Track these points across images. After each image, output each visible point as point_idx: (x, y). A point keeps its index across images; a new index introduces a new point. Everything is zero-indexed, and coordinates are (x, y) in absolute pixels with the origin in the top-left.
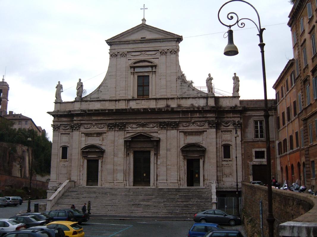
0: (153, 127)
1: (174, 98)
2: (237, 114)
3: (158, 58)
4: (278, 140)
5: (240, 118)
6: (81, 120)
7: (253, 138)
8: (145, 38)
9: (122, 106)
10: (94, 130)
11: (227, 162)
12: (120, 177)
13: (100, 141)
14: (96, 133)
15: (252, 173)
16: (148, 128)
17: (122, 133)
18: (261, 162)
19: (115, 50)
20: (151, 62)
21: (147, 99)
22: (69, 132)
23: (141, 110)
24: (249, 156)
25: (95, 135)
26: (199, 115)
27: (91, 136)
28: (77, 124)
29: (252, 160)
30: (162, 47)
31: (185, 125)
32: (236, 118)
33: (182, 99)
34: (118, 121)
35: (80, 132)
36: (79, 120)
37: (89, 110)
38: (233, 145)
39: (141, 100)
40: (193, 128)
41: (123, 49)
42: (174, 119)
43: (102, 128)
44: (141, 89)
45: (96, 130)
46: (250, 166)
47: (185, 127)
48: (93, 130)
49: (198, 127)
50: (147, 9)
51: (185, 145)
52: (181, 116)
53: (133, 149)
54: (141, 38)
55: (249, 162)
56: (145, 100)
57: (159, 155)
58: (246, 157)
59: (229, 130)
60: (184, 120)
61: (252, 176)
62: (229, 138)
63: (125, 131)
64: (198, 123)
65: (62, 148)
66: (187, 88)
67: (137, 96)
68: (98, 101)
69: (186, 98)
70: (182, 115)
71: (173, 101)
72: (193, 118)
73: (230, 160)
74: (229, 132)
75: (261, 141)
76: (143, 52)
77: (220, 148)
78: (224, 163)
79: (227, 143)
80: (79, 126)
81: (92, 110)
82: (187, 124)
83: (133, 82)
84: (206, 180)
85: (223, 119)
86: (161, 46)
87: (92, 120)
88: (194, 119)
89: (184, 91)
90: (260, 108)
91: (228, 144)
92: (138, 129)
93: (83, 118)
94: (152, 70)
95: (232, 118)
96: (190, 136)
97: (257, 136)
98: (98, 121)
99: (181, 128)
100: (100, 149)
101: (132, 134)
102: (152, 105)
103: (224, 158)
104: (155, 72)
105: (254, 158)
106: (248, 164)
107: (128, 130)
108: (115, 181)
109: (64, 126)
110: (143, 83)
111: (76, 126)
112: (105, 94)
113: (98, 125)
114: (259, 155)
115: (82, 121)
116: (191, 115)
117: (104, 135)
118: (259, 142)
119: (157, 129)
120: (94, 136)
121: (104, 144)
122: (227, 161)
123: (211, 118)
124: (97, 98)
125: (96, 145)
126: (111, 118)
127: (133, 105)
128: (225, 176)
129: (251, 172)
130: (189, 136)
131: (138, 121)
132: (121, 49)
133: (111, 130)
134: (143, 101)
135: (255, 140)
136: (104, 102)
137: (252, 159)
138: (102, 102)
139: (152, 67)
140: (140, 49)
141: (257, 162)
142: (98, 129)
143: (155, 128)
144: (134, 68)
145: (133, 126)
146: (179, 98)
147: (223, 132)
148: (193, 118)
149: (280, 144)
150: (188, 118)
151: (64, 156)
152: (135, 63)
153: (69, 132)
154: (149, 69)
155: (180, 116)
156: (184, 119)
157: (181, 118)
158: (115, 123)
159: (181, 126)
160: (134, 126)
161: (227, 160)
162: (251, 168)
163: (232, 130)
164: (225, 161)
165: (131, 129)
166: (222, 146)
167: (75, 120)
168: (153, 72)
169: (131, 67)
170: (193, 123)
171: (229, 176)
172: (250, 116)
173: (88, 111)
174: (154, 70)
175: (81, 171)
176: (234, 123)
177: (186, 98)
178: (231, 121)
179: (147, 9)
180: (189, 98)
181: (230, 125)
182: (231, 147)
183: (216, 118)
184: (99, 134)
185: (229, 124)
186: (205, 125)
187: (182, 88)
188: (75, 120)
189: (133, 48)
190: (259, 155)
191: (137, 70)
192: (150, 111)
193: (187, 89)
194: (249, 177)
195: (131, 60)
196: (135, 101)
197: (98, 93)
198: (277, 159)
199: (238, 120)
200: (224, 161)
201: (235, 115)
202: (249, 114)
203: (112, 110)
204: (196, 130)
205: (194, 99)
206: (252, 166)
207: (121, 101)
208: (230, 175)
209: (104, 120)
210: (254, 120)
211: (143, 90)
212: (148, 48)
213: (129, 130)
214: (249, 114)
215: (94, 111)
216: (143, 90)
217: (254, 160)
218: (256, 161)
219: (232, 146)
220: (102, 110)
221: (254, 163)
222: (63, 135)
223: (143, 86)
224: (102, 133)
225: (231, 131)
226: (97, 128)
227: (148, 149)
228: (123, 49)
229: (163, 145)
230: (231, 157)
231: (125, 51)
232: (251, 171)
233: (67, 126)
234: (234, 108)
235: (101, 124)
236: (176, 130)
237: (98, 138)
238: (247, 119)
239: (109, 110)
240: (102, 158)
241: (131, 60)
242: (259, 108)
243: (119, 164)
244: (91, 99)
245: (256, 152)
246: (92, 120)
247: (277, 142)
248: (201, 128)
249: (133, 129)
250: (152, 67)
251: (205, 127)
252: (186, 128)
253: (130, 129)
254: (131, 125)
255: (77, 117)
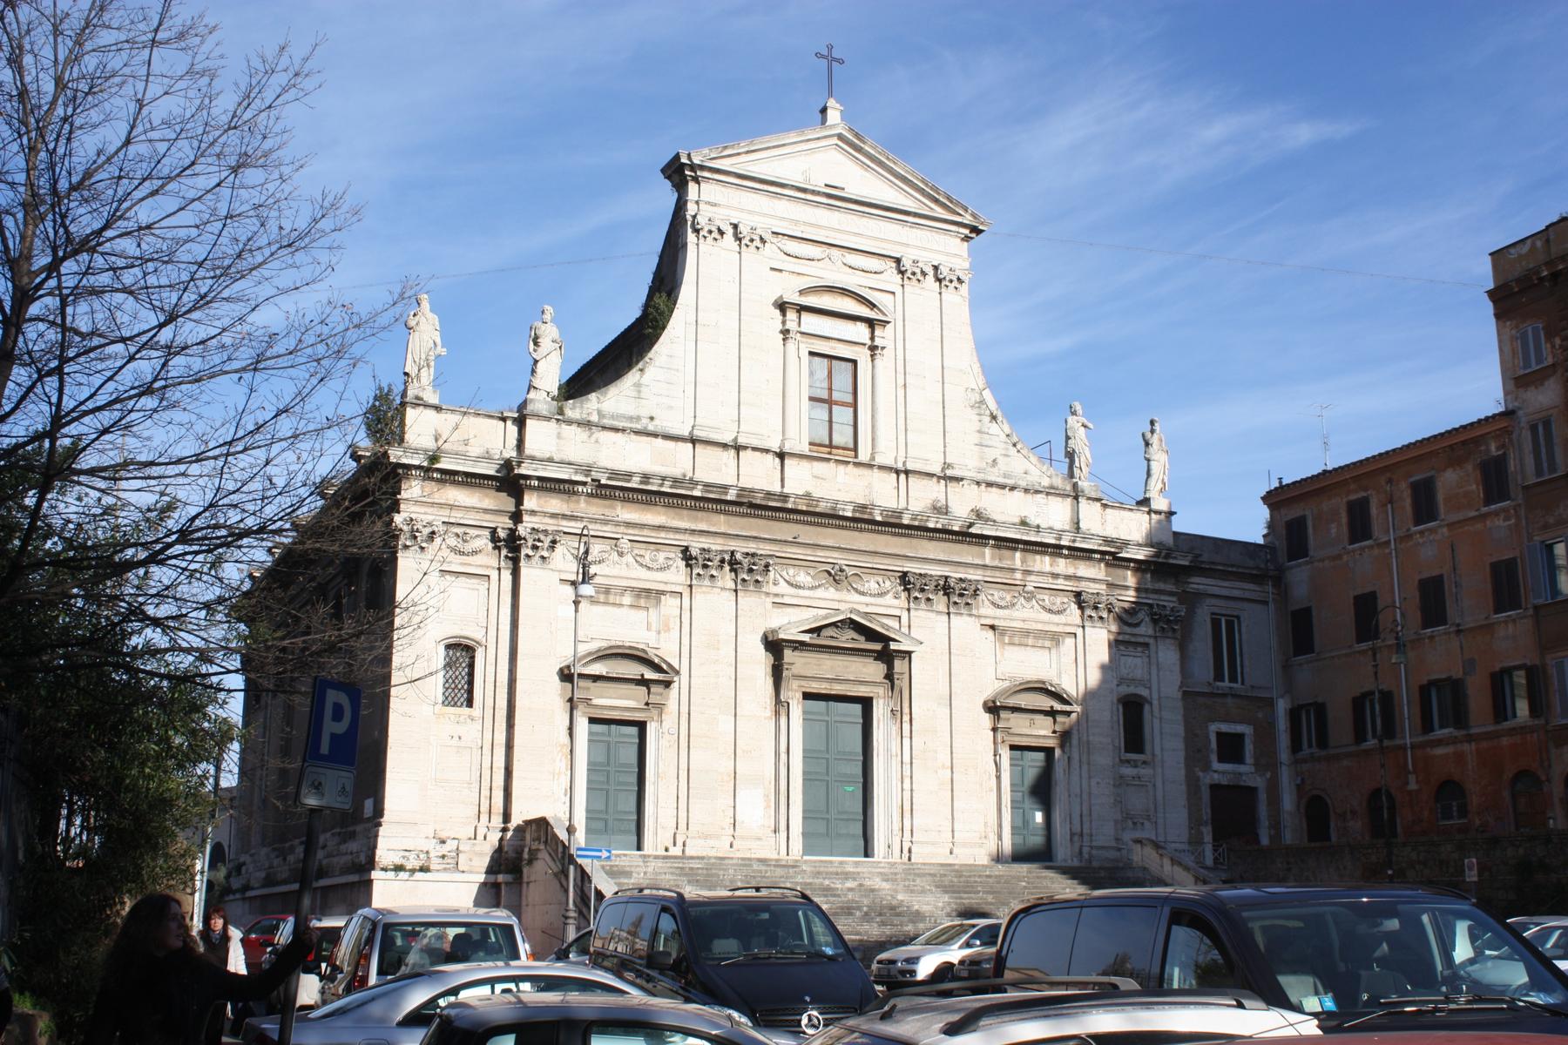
0: (881, 595)
1: (962, 479)
2: (1165, 582)
3: (893, 293)
4: (1282, 697)
5: (1174, 599)
6: (564, 516)
7: (1211, 681)
8: (843, 189)
9: (759, 475)
10: (624, 572)
11: (1136, 767)
12: (755, 810)
13: (648, 629)
14: (633, 589)
15: (1210, 816)
16: (863, 594)
17: (748, 600)
18: (1234, 773)
19: (714, 209)
20: (872, 305)
21: (856, 464)
22: (488, 567)
23: (844, 510)
24: (1199, 751)
25: (627, 600)
26: (1051, 565)
27: (606, 603)
28: (545, 532)
29: (1207, 767)
30: (910, 250)
31: (1002, 599)
32: (1163, 597)
33: (989, 489)
34: (741, 547)
35: (556, 577)
36: (554, 516)
37: (614, 474)
38: (1155, 702)
39: (832, 464)
40: (1026, 615)
41: (750, 212)
42: (961, 569)
43: (661, 569)
44: (821, 412)
45: (633, 576)
46: (1203, 788)
47: (999, 607)
48: (615, 571)
49: (1046, 616)
50: (841, 62)
51: (1007, 684)
52: (988, 561)
53: (803, 683)
54: (826, 185)
55: (1201, 774)
56: (850, 467)
57: (906, 718)
58: (1195, 756)
59: (1141, 640)
60: (999, 580)
61: (1209, 828)
62: (1138, 674)
63: (768, 594)
64: (1046, 598)
65: (448, 647)
66: (1003, 446)
67: (811, 444)
68: (637, 433)
69: (1003, 487)
70: (993, 558)
71: (957, 490)
72: (1027, 572)
73: (1144, 763)
74: (1139, 649)
75: (1232, 695)
76: (835, 252)
77: (1115, 709)
78: (1128, 771)
79: (1132, 690)
80: (554, 542)
81: (629, 476)
82: (1008, 598)
83: (803, 377)
84: (1076, 838)
85: (1123, 592)
86: (908, 245)
87: (617, 524)
88: (1033, 578)
89: (991, 454)
90: (1234, 569)
91: (1140, 696)
92: (820, 593)
93: (572, 506)
94: (872, 338)
95: (1152, 596)
96: (1016, 648)
97: (1219, 676)
98: (645, 532)
99: (985, 609)
100: (657, 668)
101: (794, 619)
102: (883, 494)
103: (1127, 751)
104: (883, 348)
105: (1214, 757)
106: (1198, 779)
107: (776, 595)
108: (723, 829)
109: (460, 530)
110: (830, 389)
111: (539, 540)
112: (671, 408)
113: (642, 552)
114: (1231, 748)
115: (564, 523)
116: (1022, 563)
117: (670, 604)
118: (1229, 700)
119: (896, 602)
120: (621, 605)
121: (662, 645)
122: (1135, 764)
123: (1092, 585)
124: (631, 419)
125: (644, 651)
126: (703, 527)
127: (803, 481)
128: (1130, 823)
129: (1207, 813)
130: (1011, 648)
131: (821, 555)
132: (742, 210)
133: (707, 582)
134: (841, 468)
135: (1218, 688)
136: (670, 444)
137: (1210, 762)
138: (659, 440)
139: (871, 323)
140: (823, 232)
141: (1223, 773)
142: (643, 573)
143: (889, 600)
144: (802, 309)
145: (798, 578)
146: (978, 483)
147: (1122, 648)
148: (1027, 572)
149: (1294, 715)
150: (1013, 570)
151: (462, 691)
152: (801, 292)
153: (488, 567)
154: (860, 332)
155: (983, 555)
156: (998, 574)
157: (985, 567)
158: (726, 552)
159: (986, 602)
160: (803, 578)
161: (1135, 761)
162: (1206, 794)
163: (1151, 641)
164: (1128, 761)
165: (792, 591)
166: (1119, 700)
167: (533, 513)
168: (877, 347)
169: (782, 306)
170: (1029, 597)
171: (1143, 824)
172: (1200, 596)
173: (609, 478)
174: (878, 342)
175: (559, 774)
176: (1160, 614)
177: (1003, 487)
178: (1151, 606)
179: (841, 62)
180: (1013, 488)
181: (1144, 623)
182: (1147, 708)
183: (1110, 585)
184: (648, 596)
185: (1141, 615)
186: (1068, 611)
187: (985, 443)
188: (533, 513)
189: (796, 222)
190: (1231, 748)
191: (811, 323)
192: (879, 518)
193: (1003, 452)
194: (1202, 834)
195: (781, 271)
196: (805, 464)
197: (635, 394)
198: (1284, 768)
199: (1172, 605)
200: (1126, 765)
201: (1161, 586)
202: (1195, 586)
203: (725, 488)
204: (1040, 627)
205: (1029, 496)
206: (1208, 790)
207: (749, 452)
208: (1146, 822)
209: (677, 530)
210: (1213, 614)
211: (830, 421)
212: (854, 239)
213: (783, 596)
214: (1195, 586)
215: (636, 479)
216: (830, 421)
217: (1216, 765)
218: (1221, 772)
219: (1151, 704)
220: (676, 482)
221: (1216, 778)
222: (448, 577)
223: (830, 402)
224: (663, 593)
225: (1146, 645)
226: (636, 565)
227: (862, 691)
228: (750, 212)
229: (925, 673)
230: (1148, 747)
231: (764, 225)
232: (1206, 813)
233: (477, 536)
234: (1167, 556)
235: (658, 550)
236: (970, 615)
237: (642, 614)
238: (1191, 600)
239: (708, 486)
240: (661, 714)
241: (781, 271)
242: (1230, 569)
243: (744, 751)
244: (599, 412)
245: (1219, 735)
246: (617, 524)
247: (1282, 706)
248: (1056, 618)
249: (801, 592)
250: (871, 323)
251: (1070, 620)
252: (1006, 612)
253: (783, 588)
254: (791, 571)
255: (539, 497)
